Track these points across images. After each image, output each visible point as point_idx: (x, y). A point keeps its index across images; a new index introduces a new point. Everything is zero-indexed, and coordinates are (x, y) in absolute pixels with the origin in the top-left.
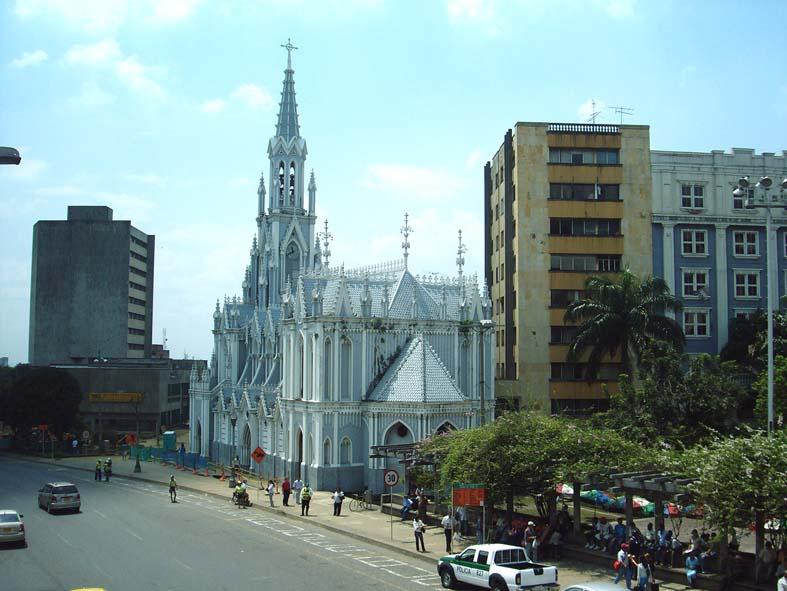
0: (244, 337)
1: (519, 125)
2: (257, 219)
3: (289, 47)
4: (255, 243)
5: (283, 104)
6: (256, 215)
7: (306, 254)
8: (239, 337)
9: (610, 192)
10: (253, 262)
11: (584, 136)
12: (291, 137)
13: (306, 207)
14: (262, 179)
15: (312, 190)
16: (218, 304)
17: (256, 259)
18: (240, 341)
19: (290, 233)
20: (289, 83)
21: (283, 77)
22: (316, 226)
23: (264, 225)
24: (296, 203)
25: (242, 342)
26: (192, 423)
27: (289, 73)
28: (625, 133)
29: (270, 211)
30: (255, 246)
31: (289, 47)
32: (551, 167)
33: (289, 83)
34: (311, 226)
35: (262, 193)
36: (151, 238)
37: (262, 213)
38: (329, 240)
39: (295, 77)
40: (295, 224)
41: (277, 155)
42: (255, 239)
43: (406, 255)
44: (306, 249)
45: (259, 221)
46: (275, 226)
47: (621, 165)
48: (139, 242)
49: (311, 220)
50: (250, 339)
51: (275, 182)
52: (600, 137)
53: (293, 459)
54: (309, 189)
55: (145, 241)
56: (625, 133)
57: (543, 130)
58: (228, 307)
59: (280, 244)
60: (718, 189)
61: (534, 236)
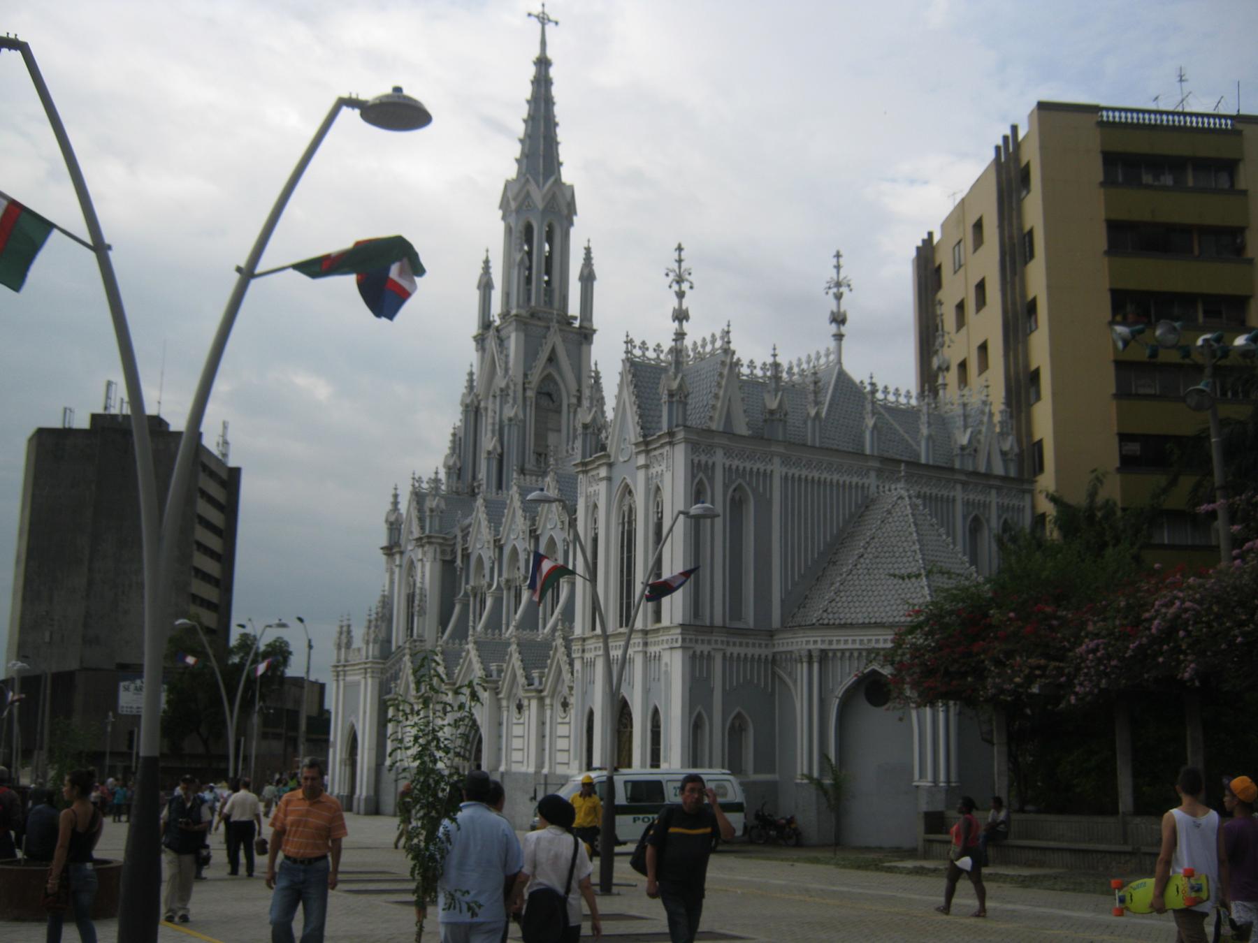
0: (454, 552)
1: (1043, 106)
2: (475, 338)
3: (543, 19)
4: (471, 381)
5: (531, 120)
6: (474, 328)
7: (574, 401)
8: (443, 552)
9: (1229, 241)
10: (466, 420)
12: (546, 178)
13: (574, 308)
14: (487, 262)
15: (588, 278)
16: (396, 496)
17: (473, 412)
18: (444, 562)
19: (544, 356)
20: (542, 82)
21: (531, 71)
22: (593, 347)
23: (492, 344)
24: (556, 304)
26: (337, 735)
27: (543, 63)
28: (1248, 130)
29: (505, 315)
30: (471, 387)
31: (543, 19)
33: (542, 82)
34: (584, 347)
35: (486, 286)
36: (235, 473)
37: (486, 324)
38: (685, 286)
39: (553, 72)
40: (555, 339)
41: (518, 211)
42: (471, 374)
43: (839, 337)
44: (573, 386)
45: (480, 340)
46: (514, 342)
47: (1244, 193)
48: (212, 474)
49: (586, 335)
50: (466, 556)
51: (518, 257)
54: (582, 278)
55: (224, 475)
56: (1248, 130)
58: (418, 497)
59: (525, 375)
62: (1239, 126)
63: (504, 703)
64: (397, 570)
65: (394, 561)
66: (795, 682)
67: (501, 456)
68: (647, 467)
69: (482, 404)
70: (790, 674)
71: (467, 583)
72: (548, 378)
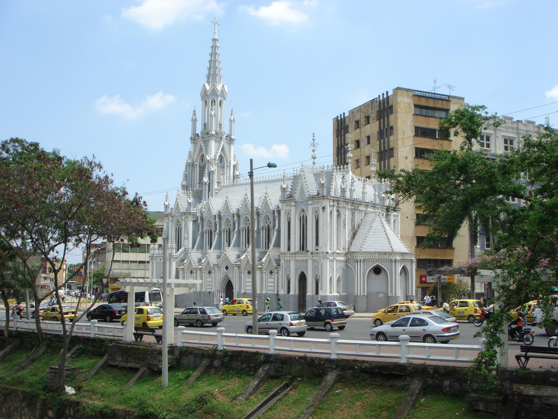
11: (432, 100)
14: (194, 111)
25: (195, 222)
30: (190, 156)
32: (415, 116)
35: (194, 121)
38: (315, 148)
42: (190, 152)
52: (440, 101)
53: (295, 292)
57: (411, 94)
60: (497, 139)
61: (407, 158)
62: (450, 99)
63: (243, 271)
64: (170, 223)
65: (169, 219)
66: (354, 267)
67: (209, 183)
68: (312, 204)
69: (195, 163)
70: (352, 265)
71: (202, 228)
72: (221, 156)
